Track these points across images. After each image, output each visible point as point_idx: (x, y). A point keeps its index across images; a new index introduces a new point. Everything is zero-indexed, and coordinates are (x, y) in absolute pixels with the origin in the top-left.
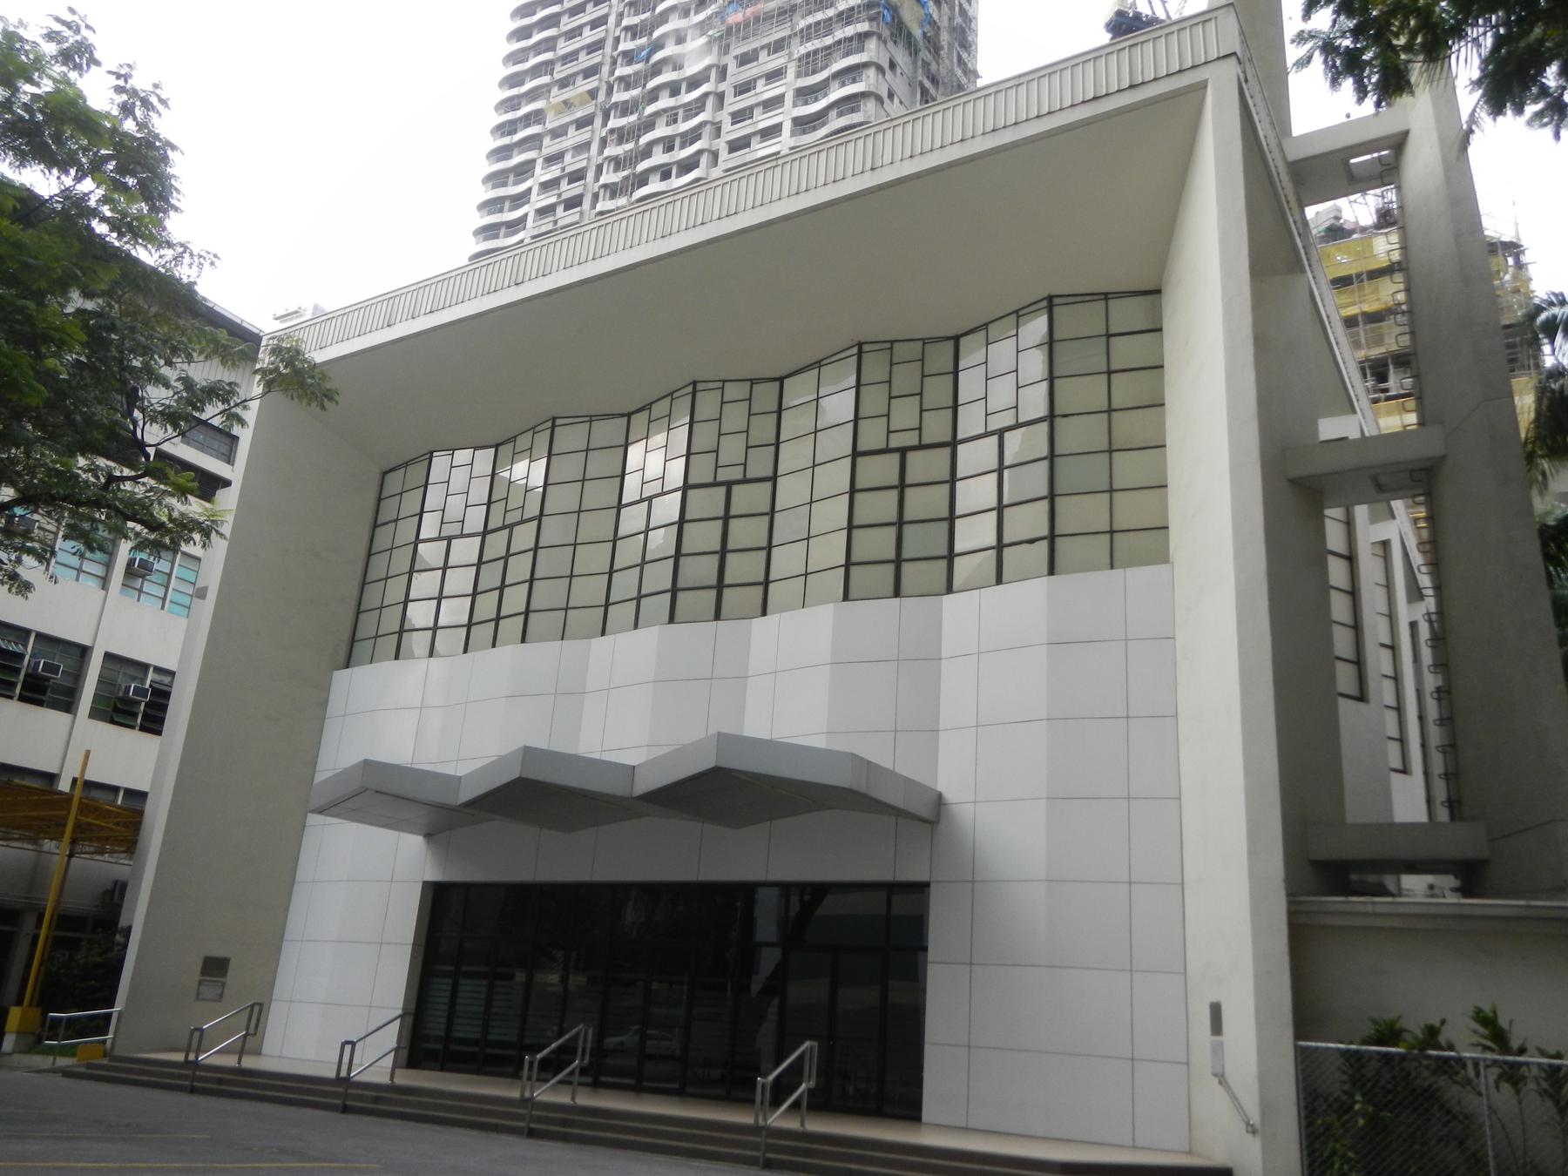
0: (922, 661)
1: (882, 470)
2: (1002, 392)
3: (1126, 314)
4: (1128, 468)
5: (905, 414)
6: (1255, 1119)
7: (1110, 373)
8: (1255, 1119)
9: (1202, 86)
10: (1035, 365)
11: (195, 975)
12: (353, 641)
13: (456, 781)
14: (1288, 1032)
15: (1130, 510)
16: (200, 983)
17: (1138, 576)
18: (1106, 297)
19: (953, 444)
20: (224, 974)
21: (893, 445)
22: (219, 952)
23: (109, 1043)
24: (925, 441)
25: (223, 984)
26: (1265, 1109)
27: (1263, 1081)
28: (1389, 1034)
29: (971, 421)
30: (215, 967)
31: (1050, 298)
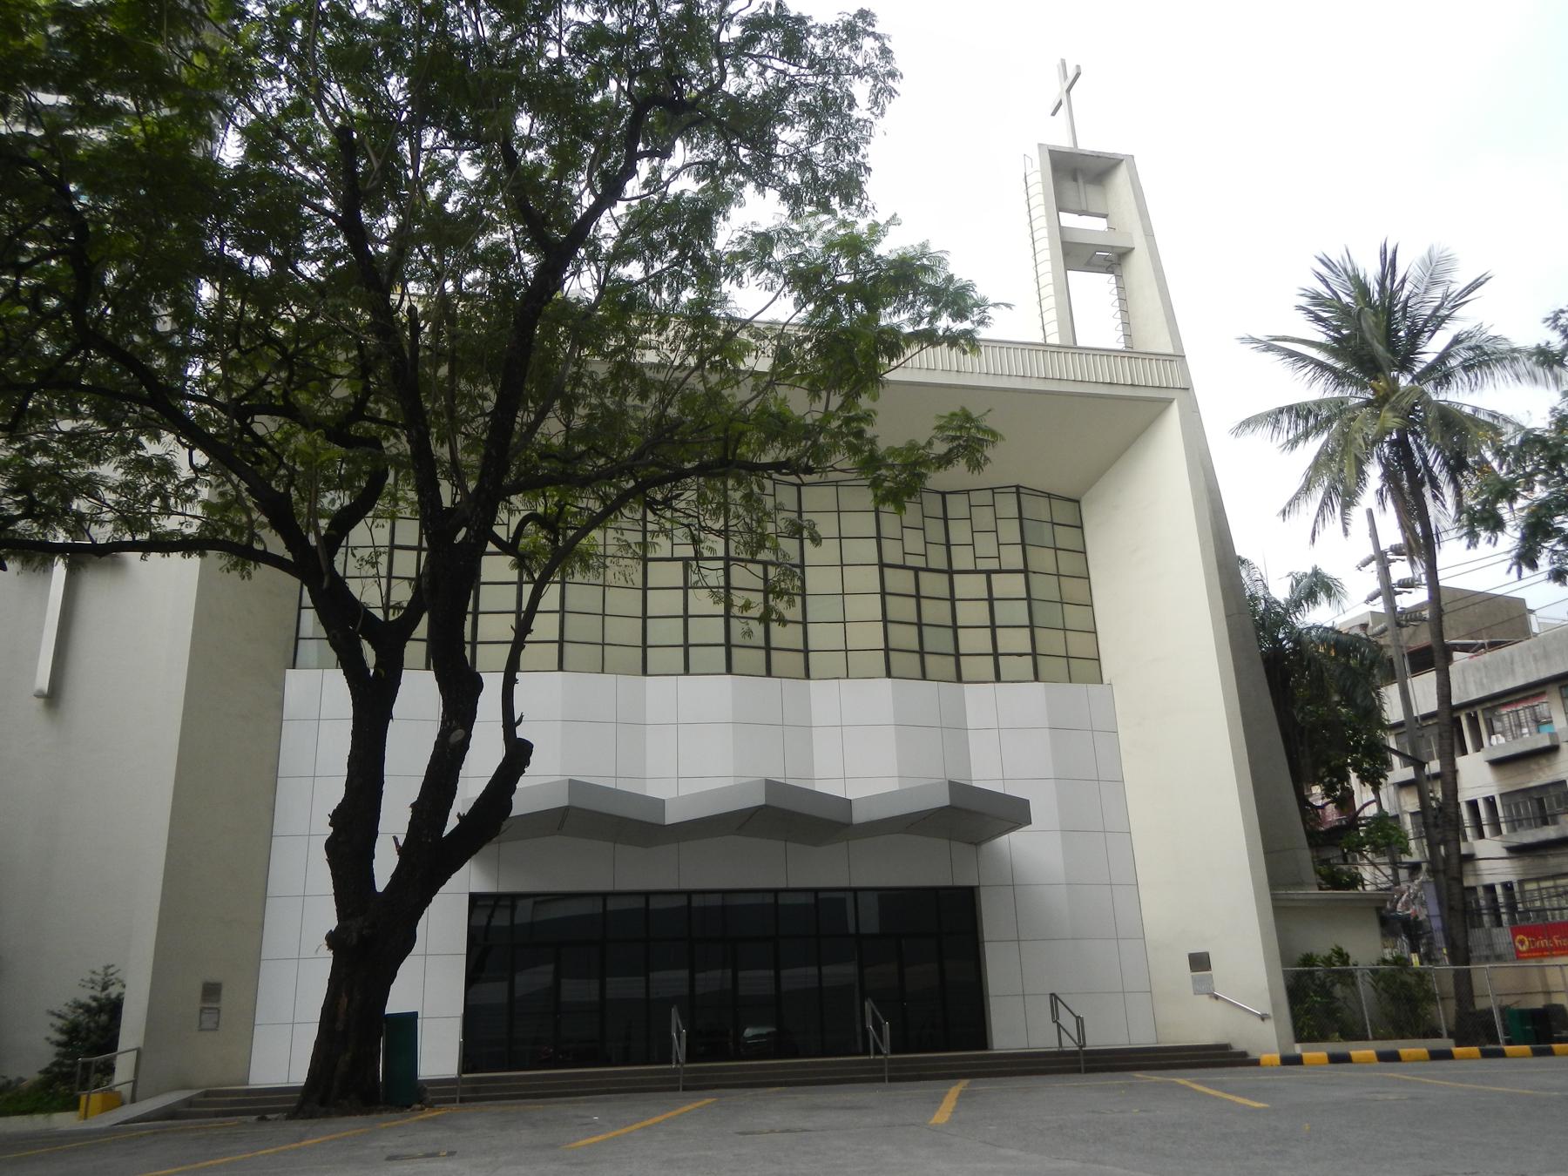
0: (955, 728)
1: (900, 581)
2: (986, 545)
3: (1063, 512)
4: (1074, 616)
5: (914, 542)
6: (1269, 1011)
7: (1056, 549)
8: (1269, 1011)
9: (1170, 401)
10: (1010, 531)
11: (197, 1003)
12: (297, 639)
13: (660, 804)
14: (1279, 963)
15: (1078, 644)
16: (202, 1010)
17: (1094, 689)
18: (1049, 496)
19: (950, 572)
20: (218, 1000)
21: (908, 563)
22: (213, 976)
23: (126, 1090)
24: (931, 565)
25: (218, 1010)
26: (1275, 1005)
27: (1271, 990)
28: (1308, 960)
29: (962, 559)
30: (211, 991)
31: (1018, 487)
